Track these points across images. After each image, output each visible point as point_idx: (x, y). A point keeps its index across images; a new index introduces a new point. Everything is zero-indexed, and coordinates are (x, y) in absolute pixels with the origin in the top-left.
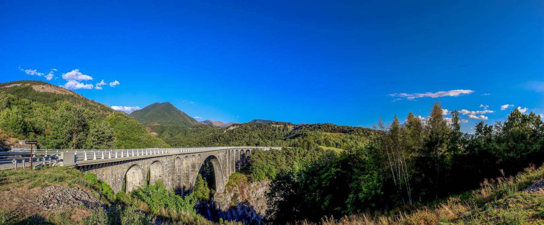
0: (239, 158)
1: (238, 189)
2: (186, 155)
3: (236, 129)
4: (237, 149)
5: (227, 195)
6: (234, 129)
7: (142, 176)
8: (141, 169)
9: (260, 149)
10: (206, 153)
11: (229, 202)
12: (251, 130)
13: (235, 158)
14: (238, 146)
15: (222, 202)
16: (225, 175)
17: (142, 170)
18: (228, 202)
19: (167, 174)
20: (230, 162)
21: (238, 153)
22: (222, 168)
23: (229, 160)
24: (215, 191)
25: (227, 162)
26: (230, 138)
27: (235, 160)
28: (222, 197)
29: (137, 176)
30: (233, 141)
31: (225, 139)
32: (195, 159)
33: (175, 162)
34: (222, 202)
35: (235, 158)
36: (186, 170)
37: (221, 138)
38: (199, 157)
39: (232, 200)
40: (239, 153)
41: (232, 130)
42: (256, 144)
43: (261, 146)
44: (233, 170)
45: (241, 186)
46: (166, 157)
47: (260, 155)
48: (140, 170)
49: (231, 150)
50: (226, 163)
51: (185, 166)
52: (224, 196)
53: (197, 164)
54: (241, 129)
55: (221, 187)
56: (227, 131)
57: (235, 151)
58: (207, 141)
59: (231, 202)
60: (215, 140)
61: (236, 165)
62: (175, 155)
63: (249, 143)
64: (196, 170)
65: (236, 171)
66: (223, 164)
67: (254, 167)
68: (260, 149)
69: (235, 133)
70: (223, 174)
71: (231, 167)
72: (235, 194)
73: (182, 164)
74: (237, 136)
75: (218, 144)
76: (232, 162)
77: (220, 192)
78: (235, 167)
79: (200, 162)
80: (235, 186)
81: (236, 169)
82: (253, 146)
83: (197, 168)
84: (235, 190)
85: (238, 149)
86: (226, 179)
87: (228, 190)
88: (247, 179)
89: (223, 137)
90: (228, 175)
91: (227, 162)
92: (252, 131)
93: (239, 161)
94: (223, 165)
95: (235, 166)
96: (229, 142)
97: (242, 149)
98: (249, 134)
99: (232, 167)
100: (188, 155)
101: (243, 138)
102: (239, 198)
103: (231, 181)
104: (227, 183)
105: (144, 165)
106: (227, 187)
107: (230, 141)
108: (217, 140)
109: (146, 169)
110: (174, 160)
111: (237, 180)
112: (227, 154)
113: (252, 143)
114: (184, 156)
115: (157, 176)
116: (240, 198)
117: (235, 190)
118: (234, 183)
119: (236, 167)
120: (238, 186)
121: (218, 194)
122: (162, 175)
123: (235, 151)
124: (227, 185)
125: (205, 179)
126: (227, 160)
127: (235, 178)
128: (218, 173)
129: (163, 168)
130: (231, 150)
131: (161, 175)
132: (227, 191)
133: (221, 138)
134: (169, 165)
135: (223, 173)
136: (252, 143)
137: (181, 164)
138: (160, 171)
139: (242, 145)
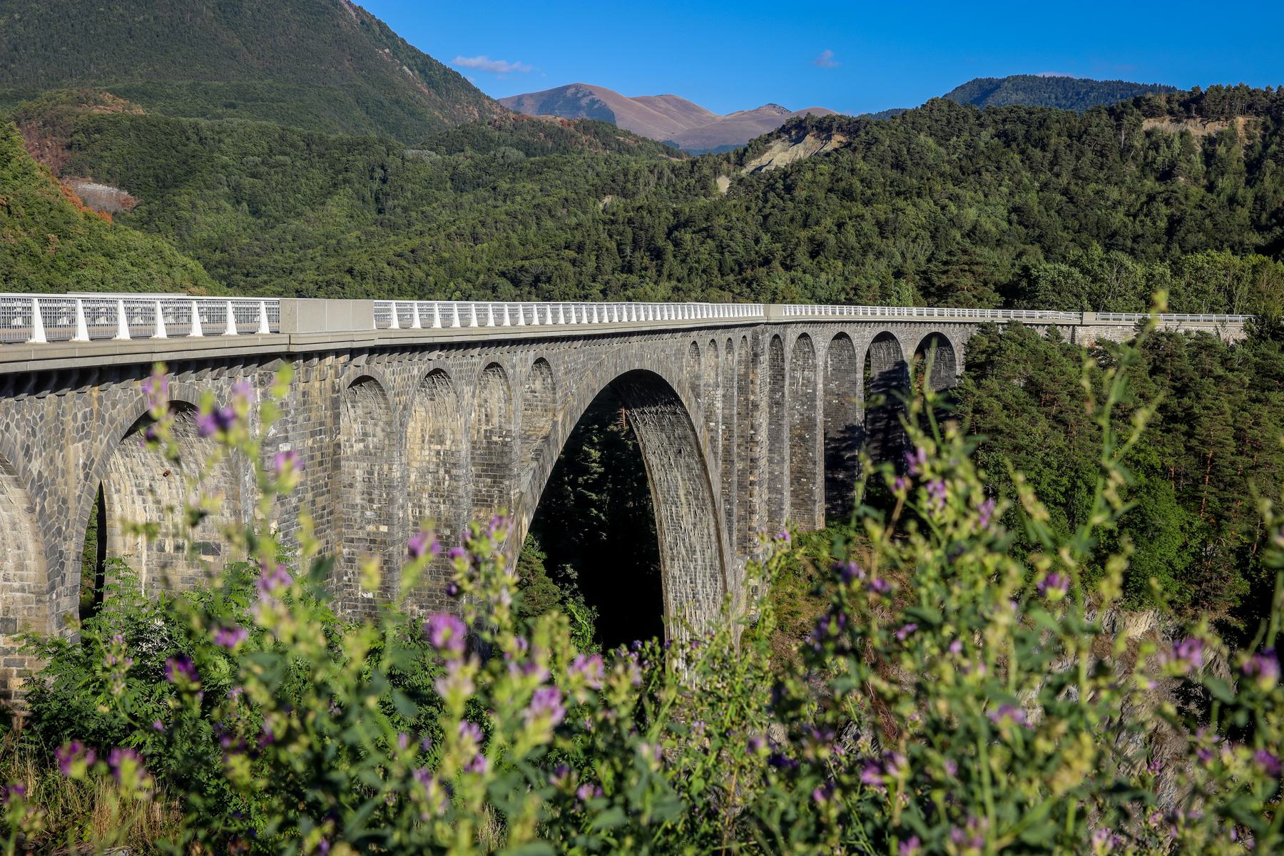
2: (435, 355)
3: (815, 160)
4: (837, 329)
6: (798, 166)
7: (31, 547)
8: (18, 483)
9: (1042, 332)
10: (594, 347)
12: (947, 168)
13: (820, 404)
14: (849, 302)
16: (745, 544)
17: (39, 488)
20: (786, 434)
21: (853, 357)
22: (717, 488)
23: (775, 420)
25: (763, 436)
26: (766, 238)
27: (820, 417)
30: (788, 268)
31: (721, 248)
32: (508, 400)
33: (337, 417)
35: (820, 404)
36: (435, 493)
38: (538, 385)
40: (860, 364)
41: (785, 175)
42: (1001, 289)
43: (1051, 305)
44: (802, 502)
46: (256, 372)
47: (1042, 378)
49: (791, 336)
50: (751, 441)
51: (420, 455)
53: (526, 438)
54: (860, 165)
56: (741, 181)
57: (822, 340)
58: (566, 264)
60: (642, 259)
61: (834, 460)
62: (338, 353)
63: (943, 281)
64: (514, 494)
65: (829, 517)
66: (727, 450)
68: (1042, 332)
69: (809, 201)
70: (725, 536)
71: (787, 480)
73: (396, 435)
74: (828, 222)
75: (665, 287)
76: (801, 440)
78: (820, 479)
79: (544, 424)
81: (828, 500)
82: (979, 301)
83: (526, 479)
85: (847, 329)
89: (708, 233)
91: (763, 436)
92: (957, 182)
93: (851, 429)
94: (728, 460)
96: (761, 272)
97: (881, 329)
98: (926, 204)
99: (799, 475)
100: (450, 361)
101: (876, 240)
103: (791, 595)
105: (57, 439)
107: (766, 262)
108: (657, 254)
109: (72, 480)
110: (335, 404)
112: (763, 371)
113: (967, 281)
114: (418, 366)
123: (822, 340)
125: (567, 579)
126: (762, 419)
128: (687, 522)
130: (791, 336)
135: (723, 526)
136: (967, 281)
137: (388, 435)
139: (884, 297)
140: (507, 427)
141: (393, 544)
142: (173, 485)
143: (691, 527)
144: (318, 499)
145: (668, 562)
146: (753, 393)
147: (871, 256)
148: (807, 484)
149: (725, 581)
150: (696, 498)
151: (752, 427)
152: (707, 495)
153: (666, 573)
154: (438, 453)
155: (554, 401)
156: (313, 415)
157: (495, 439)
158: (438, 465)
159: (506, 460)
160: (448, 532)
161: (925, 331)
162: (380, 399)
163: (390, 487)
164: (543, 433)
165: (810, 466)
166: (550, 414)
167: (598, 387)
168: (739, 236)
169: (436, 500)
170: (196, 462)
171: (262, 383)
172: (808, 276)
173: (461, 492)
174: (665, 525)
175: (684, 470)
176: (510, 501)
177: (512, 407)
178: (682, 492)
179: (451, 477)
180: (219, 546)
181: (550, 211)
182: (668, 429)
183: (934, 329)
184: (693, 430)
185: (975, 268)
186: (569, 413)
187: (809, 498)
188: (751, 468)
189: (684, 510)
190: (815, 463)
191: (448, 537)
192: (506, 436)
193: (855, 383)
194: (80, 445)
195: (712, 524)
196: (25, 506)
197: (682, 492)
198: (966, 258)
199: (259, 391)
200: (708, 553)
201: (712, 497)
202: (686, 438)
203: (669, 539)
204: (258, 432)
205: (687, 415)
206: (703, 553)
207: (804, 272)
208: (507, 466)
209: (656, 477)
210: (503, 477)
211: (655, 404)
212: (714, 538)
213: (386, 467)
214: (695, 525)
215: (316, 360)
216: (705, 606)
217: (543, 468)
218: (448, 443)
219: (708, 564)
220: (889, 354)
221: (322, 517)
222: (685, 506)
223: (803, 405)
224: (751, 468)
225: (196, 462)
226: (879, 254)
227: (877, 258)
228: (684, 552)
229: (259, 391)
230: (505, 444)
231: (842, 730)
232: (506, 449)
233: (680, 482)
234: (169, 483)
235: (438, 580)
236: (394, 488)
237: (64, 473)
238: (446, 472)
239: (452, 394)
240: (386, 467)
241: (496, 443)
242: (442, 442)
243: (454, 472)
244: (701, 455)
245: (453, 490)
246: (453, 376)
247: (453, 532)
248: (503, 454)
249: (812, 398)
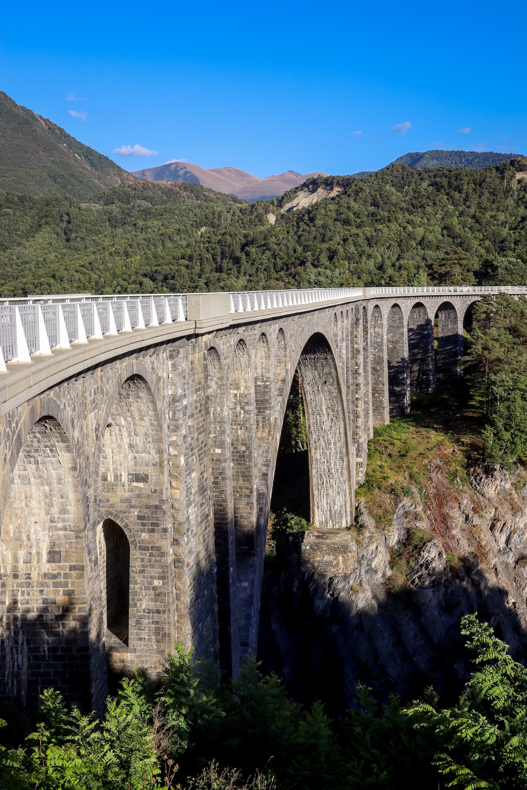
0: (406, 348)
1: (420, 509)
3: (325, 202)
4: (393, 302)
5: (371, 538)
6: (315, 207)
7: (72, 496)
8: (68, 449)
11: (380, 574)
12: (404, 205)
13: (385, 348)
14: (388, 285)
15: (346, 577)
18: (376, 572)
19: (182, 459)
21: (401, 319)
23: (365, 358)
24: (308, 520)
27: (385, 357)
28: (344, 549)
29: (34, 504)
30: (315, 266)
31: (274, 256)
32: (268, 357)
34: (346, 577)
35: (385, 348)
36: (235, 422)
37: (253, 250)
39: (392, 564)
41: (309, 212)
42: (476, 274)
43: (507, 283)
44: (378, 408)
45: (432, 491)
48: (65, 457)
50: (356, 372)
52: (353, 547)
54: (353, 204)
55: (340, 500)
56: (283, 216)
58: (183, 269)
59: (389, 573)
60: (226, 264)
67: (499, 390)
69: (324, 227)
72: (408, 531)
74: (338, 239)
75: (243, 281)
77: (330, 525)
80: (407, 492)
82: (464, 281)
83: (278, 408)
84: (406, 514)
85: (398, 302)
86: (357, 456)
87: (370, 513)
88: (460, 456)
90: (363, 439)
92: (411, 213)
95: (386, 388)
96: (300, 269)
97: (417, 301)
98: (394, 226)
101: (367, 249)
102: (432, 555)
103: (381, 467)
104: (362, 478)
106: (363, 500)
107: (303, 263)
108: (237, 261)
111: (407, 461)
115: (117, 477)
116: (434, 553)
117: (406, 514)
118: (400, 478)
119: (392, 393)
120: (420, 490)
121: (322, 535)
122: (151, 471)
123: (386, 308)
124: (361, 486)
127: (396, 449)
128: (326, 426)
129: (158, 417)
131: (142, 470)
132: (367, 519)
133: (253, 250)
134: (185, 402)
136: (457, 270)
138: (139, 440)
139: (409, 282)
140: (267, 375)
141: (225, 461)
142: (113, 433)
143: (328, 428)
144: (200, 436)
145: (313, 451)
146: (356, 343)
147: (364, 258)
148: (379, 397)
149: (349, 461)
150: (333, 411)
151: (356, 365)
152: (340, 408)
153: (312, 457)
154: (235, 395)
155: (285, 356)
156: (196, 377)
157: (259, 383)
158: (236, 404)
159: (267, 397)
160: (243, 448)
161: (441, 301)
162: (216, 362)
163: (222, 422)
164: (281, 377)
165: (381, 386)
166: (283, 365)
167: (303, 345)
168: (284, 248)
169: (235, 427)
170: (132, 416)
171: (171, 357)
172: (328, 270)
173: (252, 421)
174: (312, 428)
175: (327, 394)
176: (270, 425)
177: (270, 362)
178: (324, 408)
179: (245, 412)
180: (147, 476)
181: (170, 237)
182: (320, 369)
183: (446, 300)
184: (336, 368)
185: (461, 262)
186: (293, 364)
187: (380, 405)
188: (357, 389)
189: (325, 418)
190: (383, 384)
191: (244, 452)
192: (266, 381)
193: (403, 334)
194: (93, 414)
195: (342, 426)
196: (70, 466)
197: (324, 408)
198: (456, 256)
199: (170, 363)
200: (338, 444)
201: (343, 410)
202: (330, 374)
203: (314, 436)
204: (170, 392)
205: (333, 359)
206: (335, 444)
207: (326, 268)
208: (267, 401)
209: (308, 399)
210: (265, 408)
211: (315, 353)
212: (343, 435)
213: (219, 409)
214: (331, 427)
215: (200, 338)
216: (335, 476)
217: (284, 400)
218: (242, 388)
219: (338, 451)
220: (420, 316)
221: (202, 449)
222: (326, 416)
223: (375, 349)
224: (357, 389)
225: (132, 416)
226: (369, 256)
227: (368, 259)
228: (323, 444)
229: (170, 363)
230: (266, 387)
231: (421, 548)
232: (267, 390)
233: (324, 401)
234: (111, 432)
235: (238, 481)
236: (225, 422)
237: (87, 436)
238: (241, 408)
239: (246, 356)
240: (219, 409)
241: (260, 386)
242: (238, 388)
243: (247, 408)
244: (339, 384)
245: (247, 420)
246: (247, 343)
247: (248, 448)
248: (264, 393)
249: (381, 345)
